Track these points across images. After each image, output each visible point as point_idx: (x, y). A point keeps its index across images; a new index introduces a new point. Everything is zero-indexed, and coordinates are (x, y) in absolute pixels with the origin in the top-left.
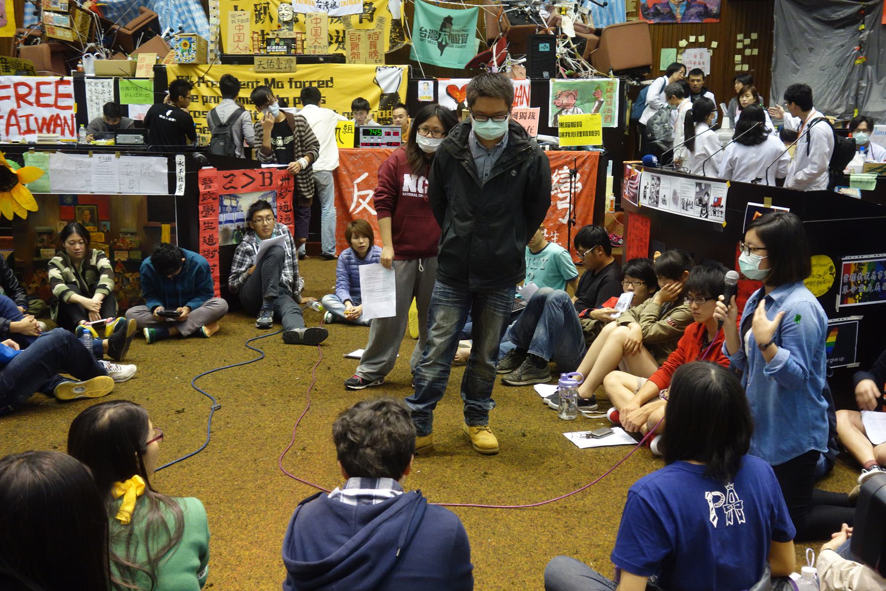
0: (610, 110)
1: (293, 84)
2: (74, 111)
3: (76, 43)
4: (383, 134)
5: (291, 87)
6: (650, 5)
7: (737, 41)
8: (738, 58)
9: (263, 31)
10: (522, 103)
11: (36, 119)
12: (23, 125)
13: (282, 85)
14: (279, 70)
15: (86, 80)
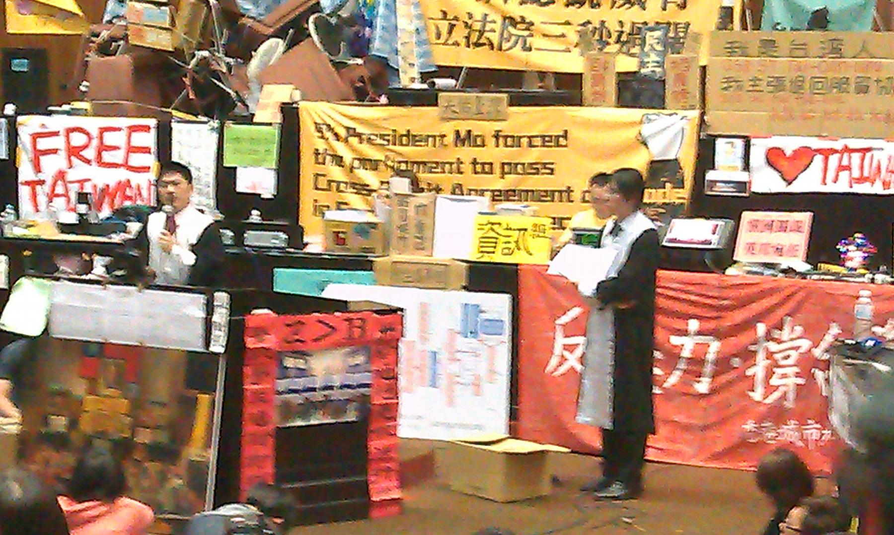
1: (501, 140)
2: (152, 176)
13: (483, 141)
14: (481, 116)
15: (174, 125)
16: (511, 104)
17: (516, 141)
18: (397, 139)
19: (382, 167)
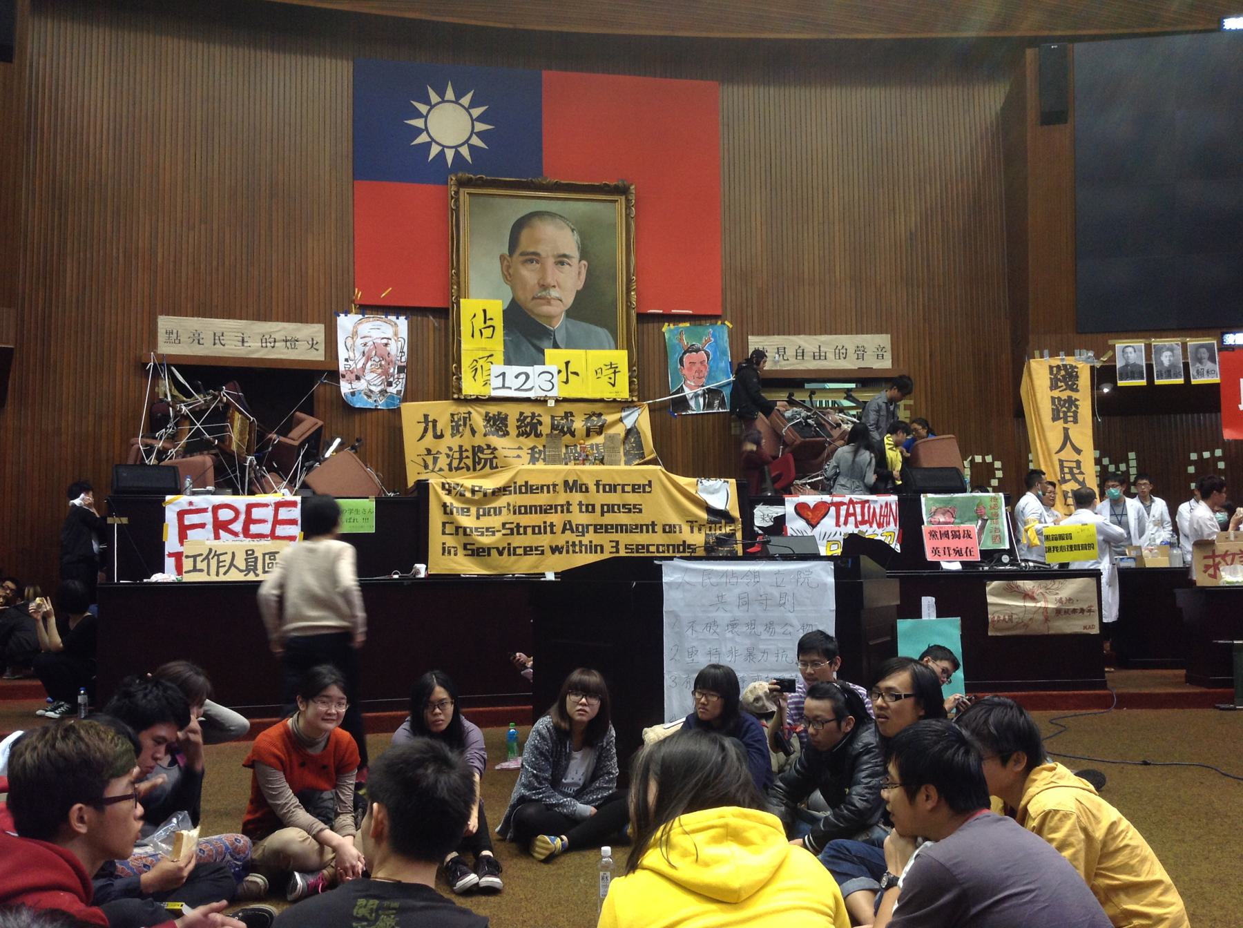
0: (997, 530)
9: (461, 447)
10: (888, 523)
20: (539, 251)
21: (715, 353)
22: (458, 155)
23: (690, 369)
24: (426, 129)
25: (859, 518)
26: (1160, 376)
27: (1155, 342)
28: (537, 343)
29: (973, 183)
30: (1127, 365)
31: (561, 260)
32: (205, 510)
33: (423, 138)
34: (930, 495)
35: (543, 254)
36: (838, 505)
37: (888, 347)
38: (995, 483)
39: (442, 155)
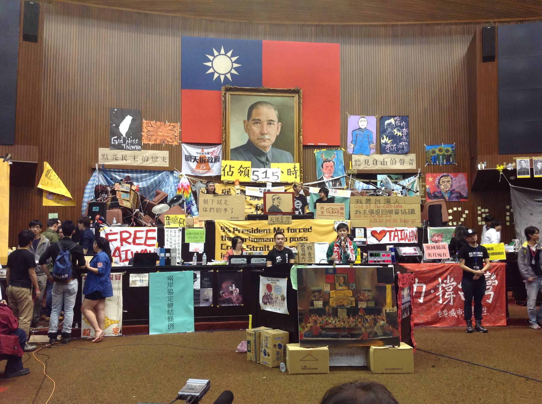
3: (131, 210)
4: (381, 255)
5: (288, 232)
6: (432, 193)
7: (477, 210)
8: (479, 218)
11: (132, 252)
12: (123, 256)
14: (282, 223)
15: (165, 229)
16: (293, 219)
17: (295, 230)
18: (253, 231)
19: (247, 241)
20: (260, 118)
21: (337, 163)
22: (226, 78)
23: (326, 169)
24: (212, 67)
25: (400, 237)
26: (537, 173)
27: (534, 158)
28: (259, 158)
29: (453, 87)
30: (522, 168)
31: (270, 122)
32: (116, 233)
33: (211, 71)
34: (431, 228)
35: (262, 120)
36: (390, 232)
37: (415, 159)
38: (462, 220)
39: (219, 78)
